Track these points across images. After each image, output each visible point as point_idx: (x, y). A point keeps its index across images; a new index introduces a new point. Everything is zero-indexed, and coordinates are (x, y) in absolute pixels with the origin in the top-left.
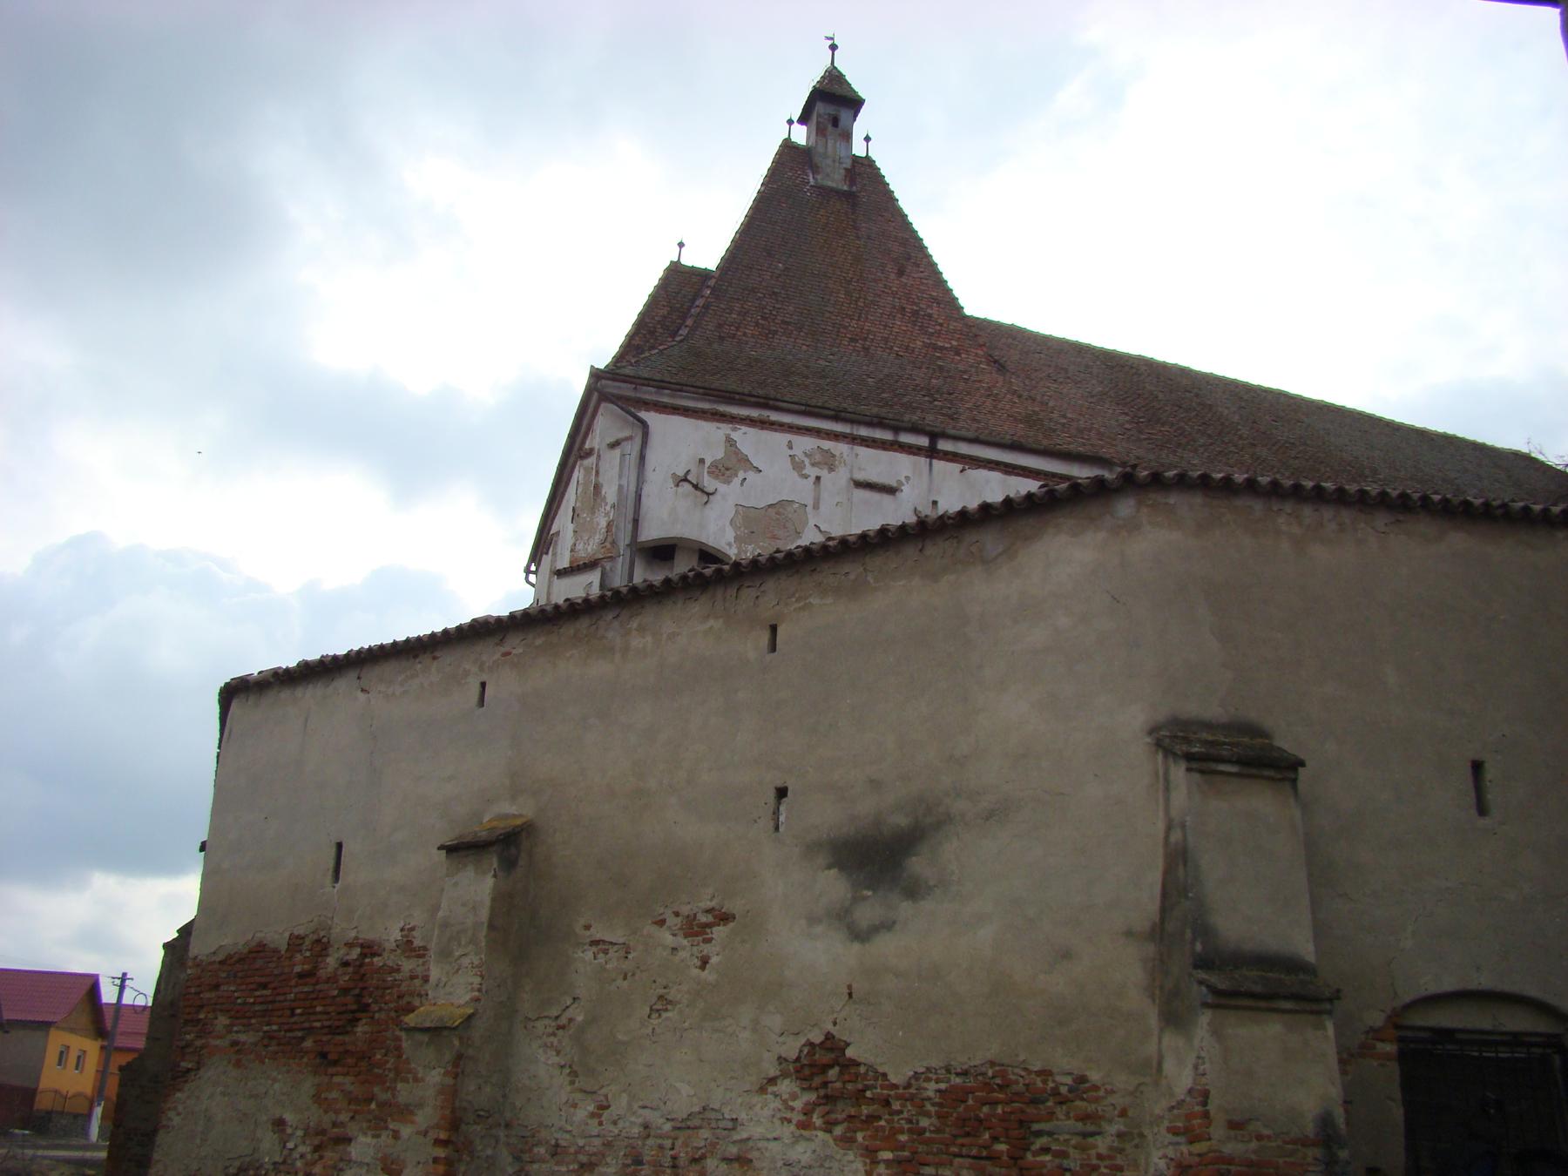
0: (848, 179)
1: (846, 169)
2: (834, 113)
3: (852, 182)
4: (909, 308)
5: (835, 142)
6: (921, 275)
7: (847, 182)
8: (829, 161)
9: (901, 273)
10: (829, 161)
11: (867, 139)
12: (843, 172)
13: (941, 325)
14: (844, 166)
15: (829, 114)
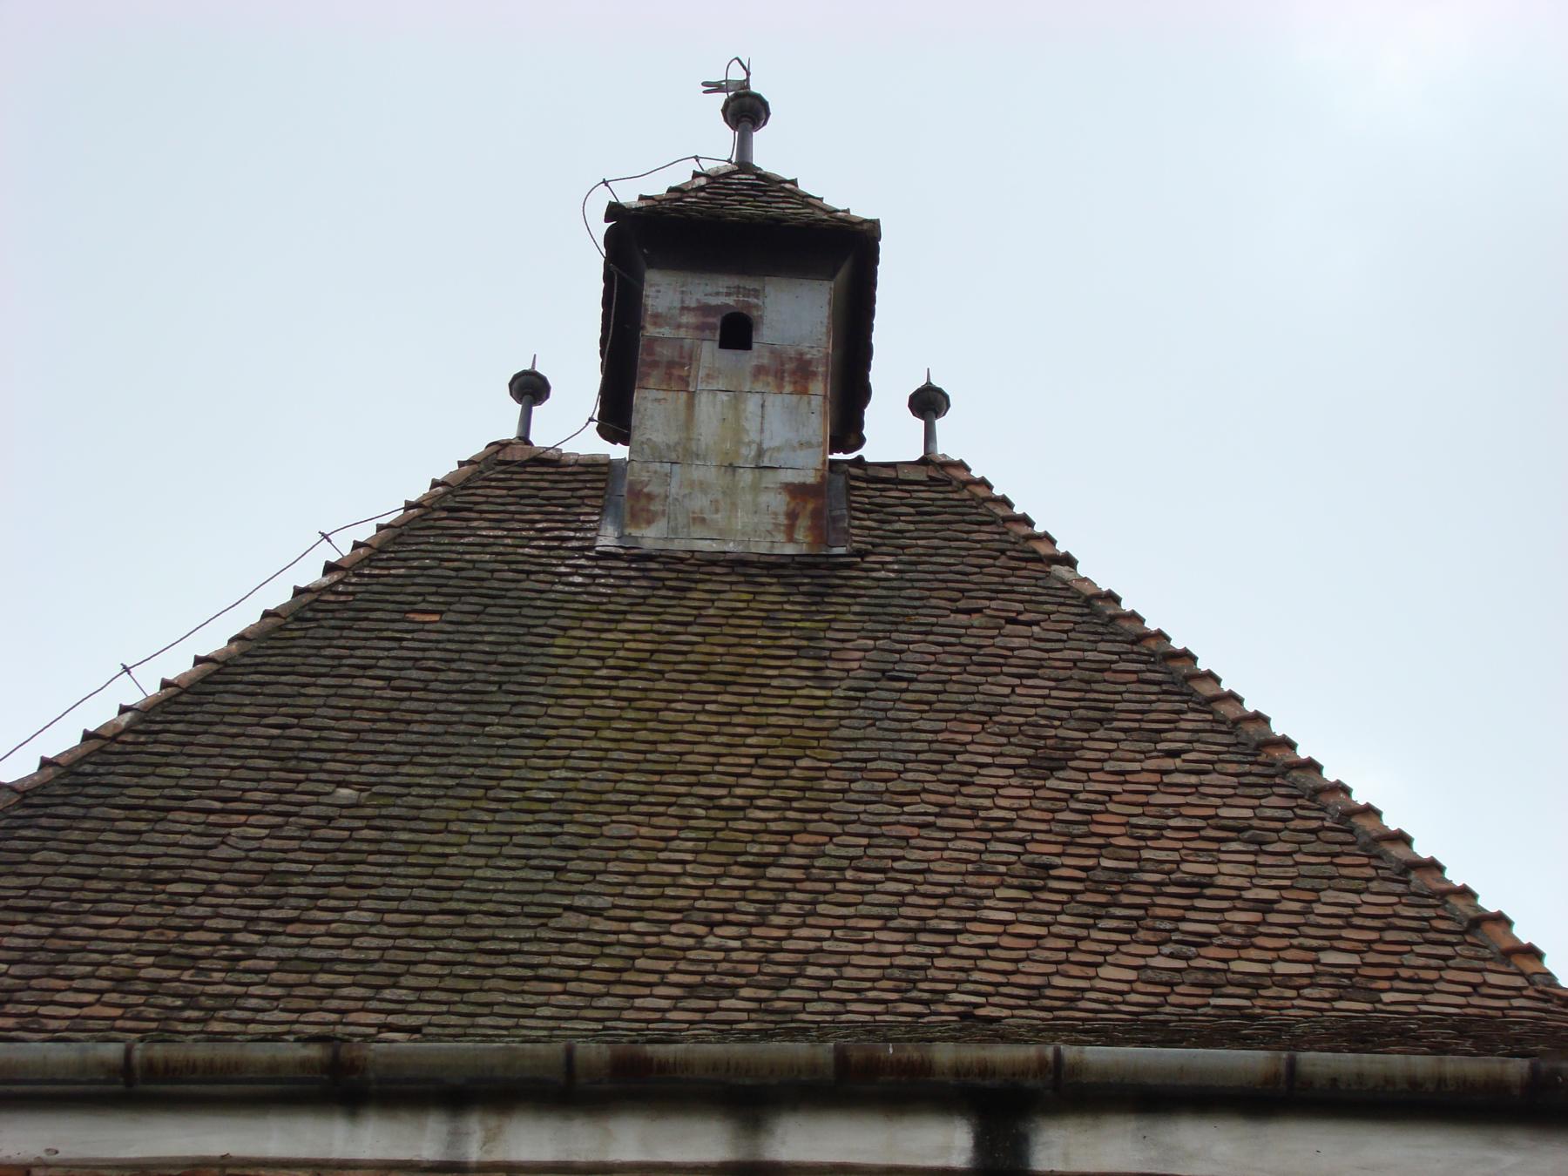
0: (804, 522)
1: (797, 491)
2: (730, 301)
3: (823, 527)
4: (1068, 866)
5: (737, 395)
6: (1168, 763)
7: (800, 535)
8: (706, 472)
9: (1047, 762)
10: (706, 472)
11: (928, 403)
12: (778, 502)
13: (1266, 906)
14: (790, 477)
15: (704, 309)
